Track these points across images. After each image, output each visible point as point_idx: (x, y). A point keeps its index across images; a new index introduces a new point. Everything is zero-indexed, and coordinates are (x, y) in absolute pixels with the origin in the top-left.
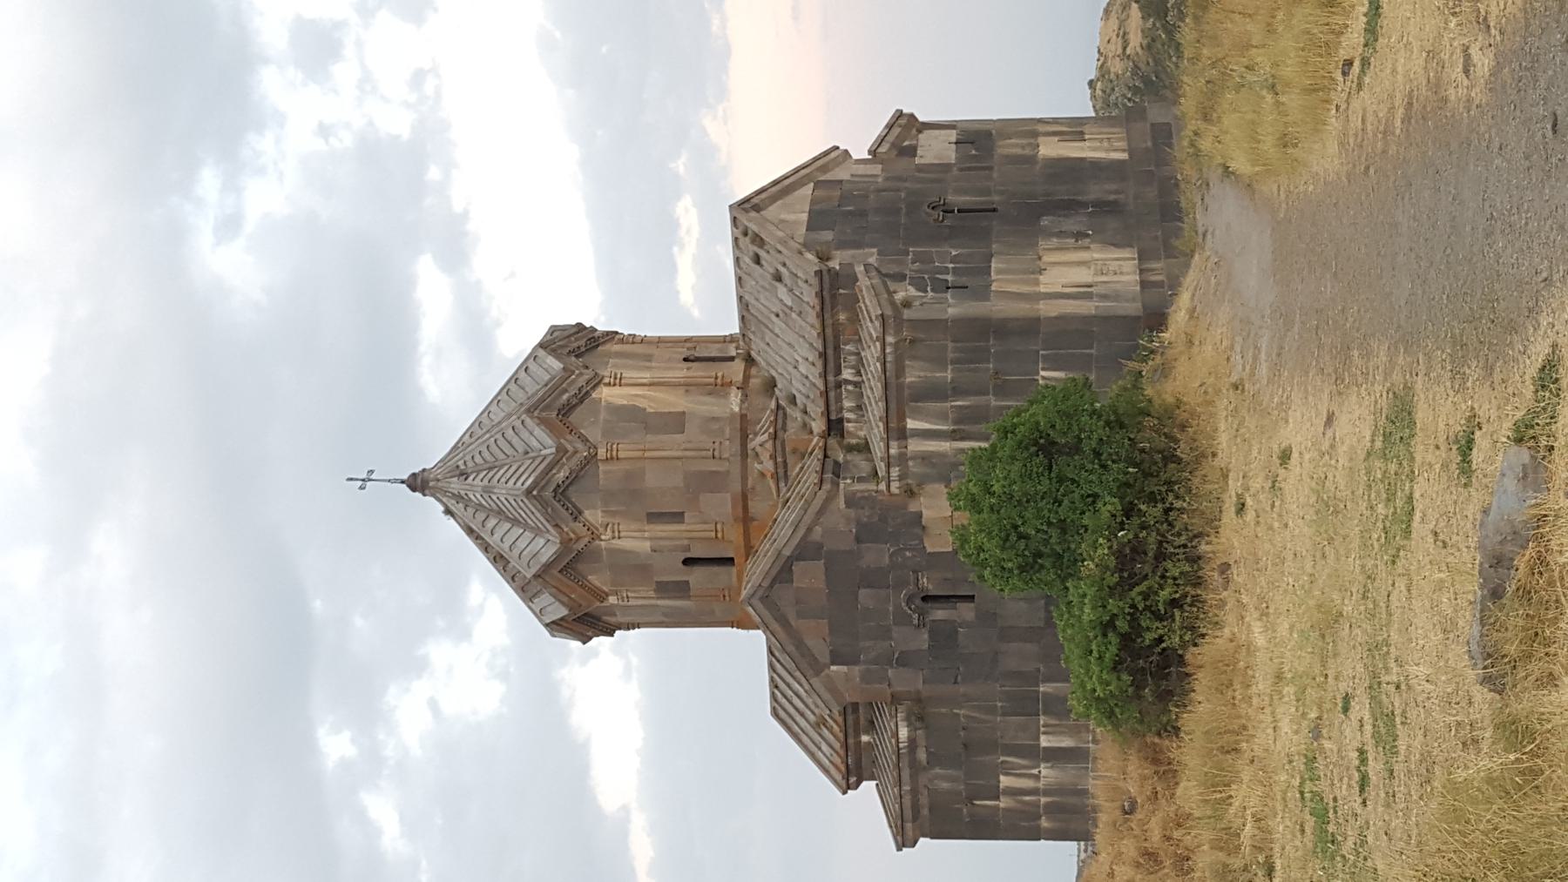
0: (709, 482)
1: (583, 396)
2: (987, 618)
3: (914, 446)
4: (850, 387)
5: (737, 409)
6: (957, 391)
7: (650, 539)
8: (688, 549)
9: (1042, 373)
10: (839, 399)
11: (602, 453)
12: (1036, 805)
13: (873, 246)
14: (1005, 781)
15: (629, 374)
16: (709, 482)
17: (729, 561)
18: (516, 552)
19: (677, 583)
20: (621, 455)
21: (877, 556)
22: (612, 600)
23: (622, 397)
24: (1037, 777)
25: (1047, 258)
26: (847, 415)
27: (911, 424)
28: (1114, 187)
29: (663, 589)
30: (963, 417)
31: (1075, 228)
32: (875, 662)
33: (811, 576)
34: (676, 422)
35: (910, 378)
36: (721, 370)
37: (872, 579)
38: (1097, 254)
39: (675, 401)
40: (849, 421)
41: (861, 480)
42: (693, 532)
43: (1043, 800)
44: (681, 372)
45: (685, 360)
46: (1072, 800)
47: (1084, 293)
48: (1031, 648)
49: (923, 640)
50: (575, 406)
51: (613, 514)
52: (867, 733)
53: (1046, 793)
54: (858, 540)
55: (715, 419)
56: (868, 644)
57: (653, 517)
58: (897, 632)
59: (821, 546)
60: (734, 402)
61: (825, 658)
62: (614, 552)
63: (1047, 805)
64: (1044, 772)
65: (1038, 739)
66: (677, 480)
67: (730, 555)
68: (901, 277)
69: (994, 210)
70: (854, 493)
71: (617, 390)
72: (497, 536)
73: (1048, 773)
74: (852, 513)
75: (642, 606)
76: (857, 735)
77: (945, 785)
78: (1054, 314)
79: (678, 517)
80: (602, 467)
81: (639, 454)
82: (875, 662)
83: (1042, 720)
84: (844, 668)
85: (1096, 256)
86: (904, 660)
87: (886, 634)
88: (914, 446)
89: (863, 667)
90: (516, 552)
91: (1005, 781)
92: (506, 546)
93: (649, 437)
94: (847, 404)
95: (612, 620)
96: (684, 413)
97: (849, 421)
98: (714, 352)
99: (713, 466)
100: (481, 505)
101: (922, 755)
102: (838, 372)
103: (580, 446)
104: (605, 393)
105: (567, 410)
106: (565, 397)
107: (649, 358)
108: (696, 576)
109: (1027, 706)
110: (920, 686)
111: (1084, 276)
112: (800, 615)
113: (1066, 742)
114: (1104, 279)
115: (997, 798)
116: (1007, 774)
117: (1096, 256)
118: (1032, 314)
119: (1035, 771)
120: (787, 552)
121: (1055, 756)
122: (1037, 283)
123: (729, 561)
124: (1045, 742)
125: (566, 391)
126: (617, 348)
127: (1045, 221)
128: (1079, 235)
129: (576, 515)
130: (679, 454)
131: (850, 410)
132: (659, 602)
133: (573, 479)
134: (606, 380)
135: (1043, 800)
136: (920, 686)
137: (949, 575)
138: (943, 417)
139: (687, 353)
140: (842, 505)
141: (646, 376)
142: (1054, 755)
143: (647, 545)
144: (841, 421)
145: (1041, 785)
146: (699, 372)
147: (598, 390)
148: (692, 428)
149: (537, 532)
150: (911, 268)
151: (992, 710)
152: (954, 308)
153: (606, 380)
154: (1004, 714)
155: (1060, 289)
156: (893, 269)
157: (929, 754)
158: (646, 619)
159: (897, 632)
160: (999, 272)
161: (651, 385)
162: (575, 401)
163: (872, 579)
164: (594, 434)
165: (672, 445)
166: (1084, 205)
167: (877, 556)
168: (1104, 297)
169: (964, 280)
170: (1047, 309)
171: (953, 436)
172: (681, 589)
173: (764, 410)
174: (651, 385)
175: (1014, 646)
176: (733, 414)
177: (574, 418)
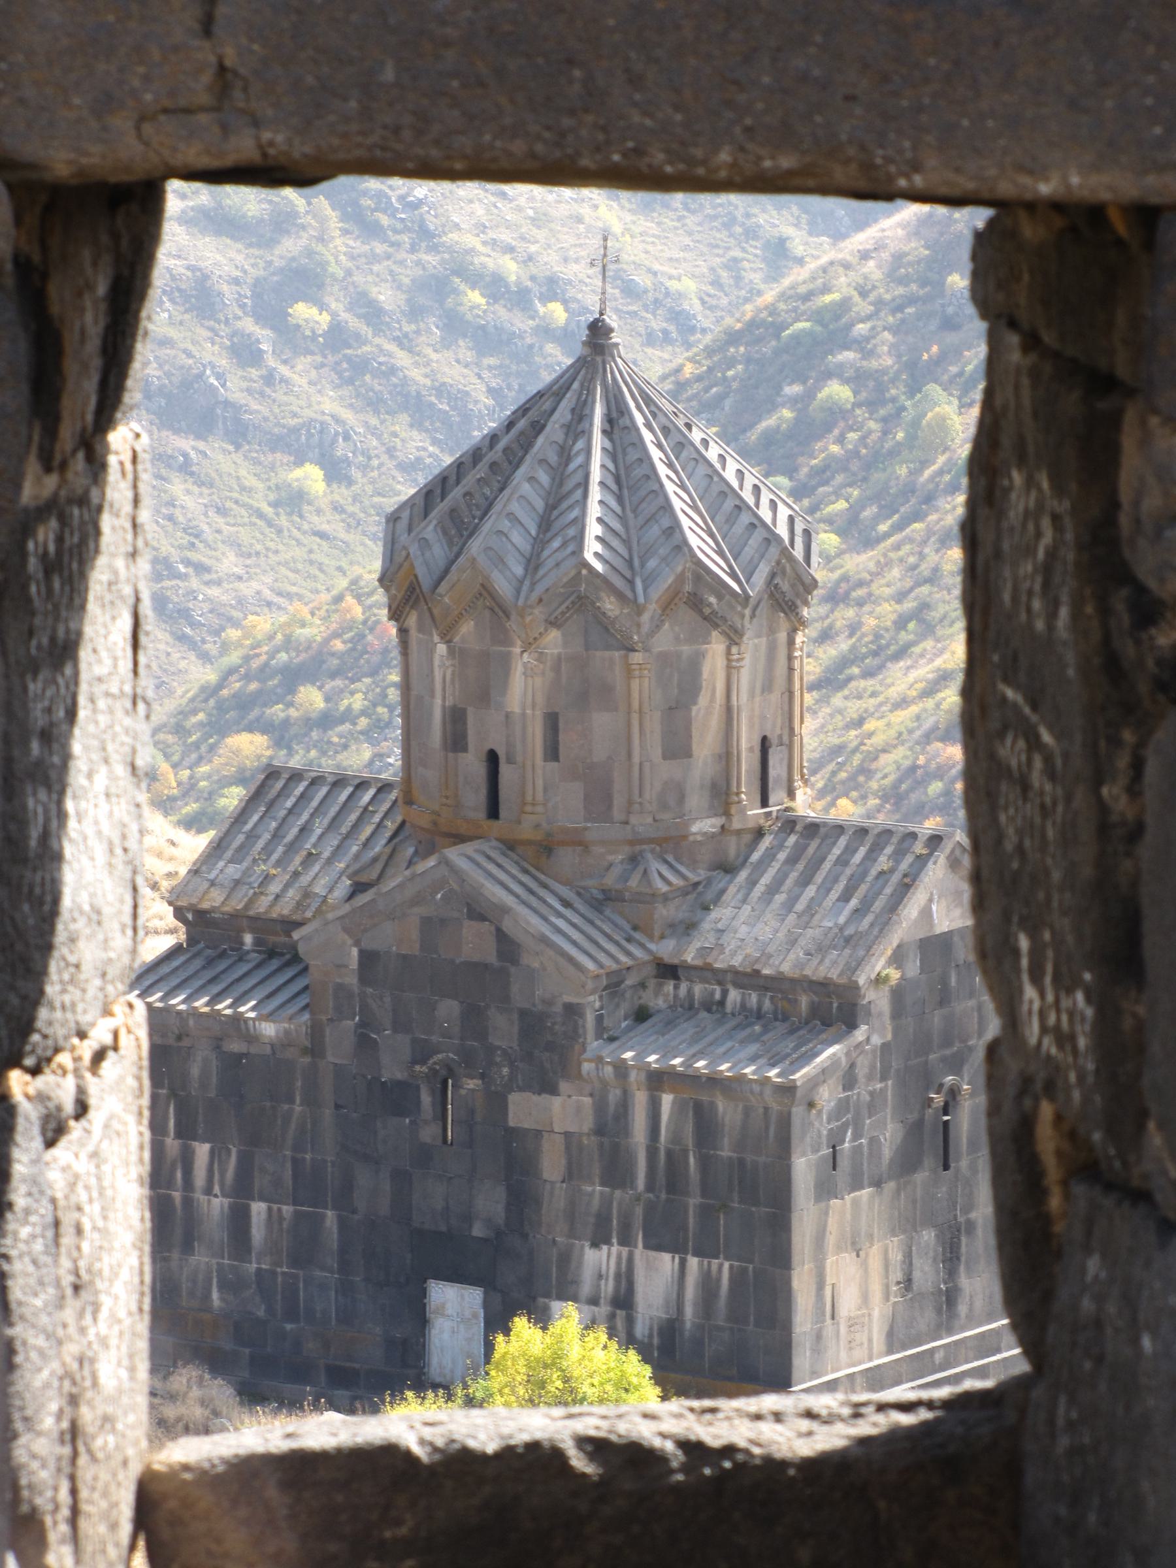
0: (599, 798)
1: (712, 620)
2: (424, 1156)
3: (640, 1099)
4: (718, 996)
5: (694, 828)
6: (705, 1163)
7: (524, 715)
8: (510, 761)
9: (726, 1265)
10: (704, 981)
11: (637, 658)
12: (170, 1184)
13: (895, 1033)
14: (202, 1151)
15: (744, 677)
16: (599, 798)
17: (493, 812)
18: (505, 525)
19: (464, 736)
20: (635, 684)
21: (504, 1031)
22: (442, 649)
23: (713, 673)
24: (208, 1191)
25: (874, 1255)
26: (684, 987)
27: (667, 1100)
28: (979, 1304)
29: (456, 718)
30: (675, 1161)
31: (917, 1275)
32: (364, 1008)
33: (474, 944)
34: (678, 747)
35: (721, 1105)
36: (747, 794)
37: (474, 1020)
38: (878, 1315)
39: (705, 745)
40: (676, 987)
41: (599, 1019)
42: (535, 782)
43: (177, 1195)
44: (746, 741)
45: (764, 741)
46: (178, 1232)
47: (827, 1311)
48: (384, 1207)
49: (392, 1071)
50: (700, 612)
51: (557, 669)
52: (258, 942)
53: (188, 1202)
54: (523, 1013)
55: (681, 799)
56: (387, 999)
57: (552, 722)
58: (403, 1041)
59: (515, 961)
60: (704, 826)
61: (369, 944)
62: (505, 662)
63: (169, 1198)
64: (216, 1202)
65: (262, 1198)
66: (600, 754)
67: (503, 812)
68: (849, 1081)
69: (946, 1167)
70: (582, 1015)
71: (721, 663)
72: (526, 488)
73: (216, 1206)
74: (558, 1008)
75: (432, 671)
76: (252, 930)
77: (195, 1071)
78: (795, 1284)
79: (553, 752)
80: (617, 655)
81: (635, 705)
82: (364, 1008)
83: (287, 1210)
84: (354, 963)
85: (876, 1313)
86: (365, 1043)
87: (400, 1025)
88: (640, 1099)
89: (356, 991)
90: (505, 525)
91: (202, 1151)
92: (515, 507)
93: (657, 715)
94: (698, 989)
95: (412, 621)
96: (690, 756)
97: (676, 987)
98: (776, 769)
99: (619, 801)
100: (569, 460)
101: (236, 1047)
102: (737, 985)
103: (645, 628)
104: (716, 647)
105: (695, 603)
106: (713, 600)
107: (768, 687)
108: (472, 764)
109: (308, 1187)
110: (331, 1059)
111: (848, 1304)
112: (426, 922)
113: (257, 1233)
114: (843, 1329)
115: (179, 1135)
116: (212, 1152)
117: (876, 1313)
118: (796, 1258)
119: (217, 1189)
120: (507, 925)
121: (239, 1219)
122: (839, 1249)
123: (493, 812)
124: (258, 1209)
125: (720, 598)
126: (782, 636)
127: (928, 1236)
128: (907, 1283)
129: (553, 623)
130: (636, 759)
131: (690, 992)
132: (438, 701)
133: (604, 624)
134: (734, 650)
135: (177, 1195)
136: (331, 1059)
137: (478, 1118)
138: (676, 1138)
139: (774, 740)
140: (568, 999)
141: (741, 698)
142: (239, 1219)
143: (517, 710)
144: (676, 977)
145: (199, 1196)
146: (747, 763)
147: (722, 638)
148: (667, 770)
149: (533, 563)
150: (862, 1091)
151: (298, 1147)
152: (804, 1167)
153: (734, 650)
154: (295, 1161)
155: (829, 1280)
156: (861, 1072)
157: (241, 1056)
158: (414, 668)
159: (403, 1040)
160: (856, 1203)
161: (728, 709)
162: (707, 611)
163: (474, 1020)
164: (664, 641)
165: (649, 743)
166: (952, 1273)
167: (504, 1031)
168: (819, 1337)
169: (844, 1163)
170: (801, 1281)
171: (652, 1152)
172: (456, 741)
173: (693, 864)
174: (728, 709)
175: (387, 1186)
176: (687, 825)
177: (685, 614)
